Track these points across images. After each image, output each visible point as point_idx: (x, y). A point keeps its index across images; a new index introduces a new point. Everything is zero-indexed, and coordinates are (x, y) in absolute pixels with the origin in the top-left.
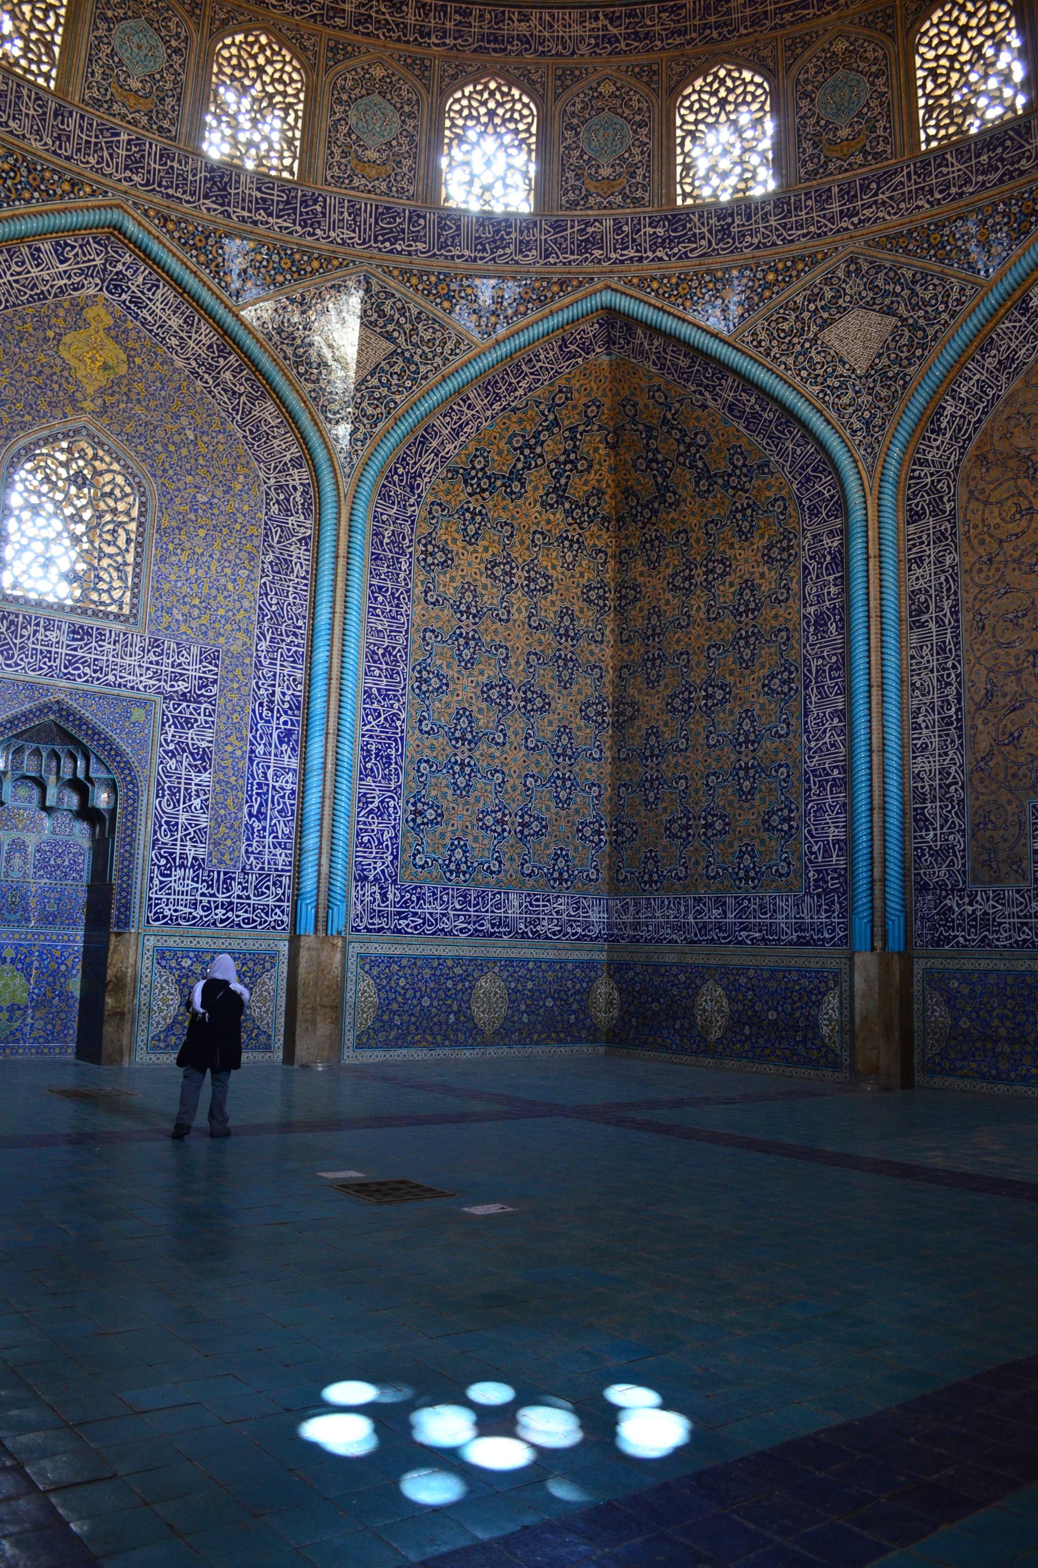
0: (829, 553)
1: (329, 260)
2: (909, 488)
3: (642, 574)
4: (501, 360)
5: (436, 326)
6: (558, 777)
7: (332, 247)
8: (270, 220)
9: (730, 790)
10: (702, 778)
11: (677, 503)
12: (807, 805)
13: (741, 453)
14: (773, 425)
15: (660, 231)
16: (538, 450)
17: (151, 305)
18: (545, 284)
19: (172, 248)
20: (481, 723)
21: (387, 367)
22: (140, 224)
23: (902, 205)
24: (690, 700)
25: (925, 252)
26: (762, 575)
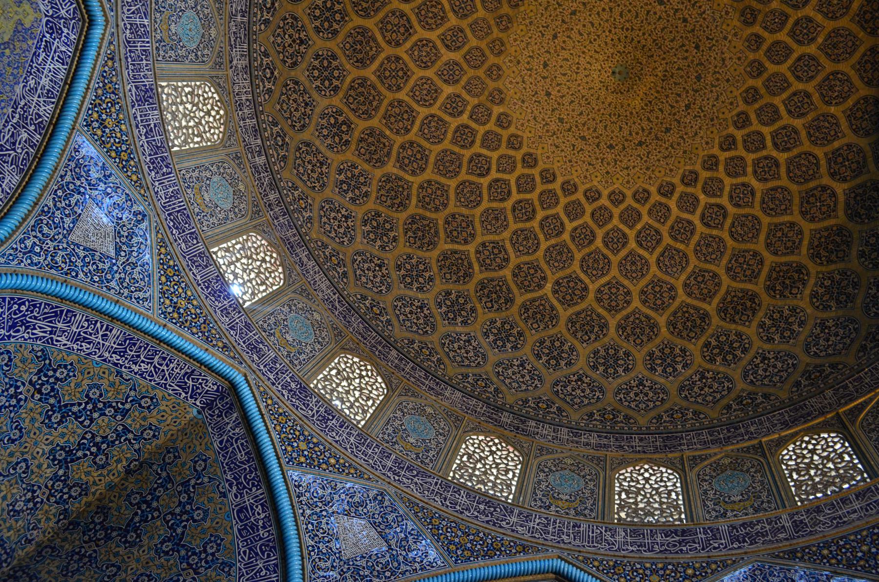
1: (141, 186)
4: (154, 336)
7: (150, 185)
8: (143, 137)
11: (132, 545)
13: (219, 545)
15: (293, 385)
16: (95, 415)
17: (50, 59)
18: (217, 336)
19: (98, 66)
22: (102, 39)
23: (426, 492)
25: (426, 523)
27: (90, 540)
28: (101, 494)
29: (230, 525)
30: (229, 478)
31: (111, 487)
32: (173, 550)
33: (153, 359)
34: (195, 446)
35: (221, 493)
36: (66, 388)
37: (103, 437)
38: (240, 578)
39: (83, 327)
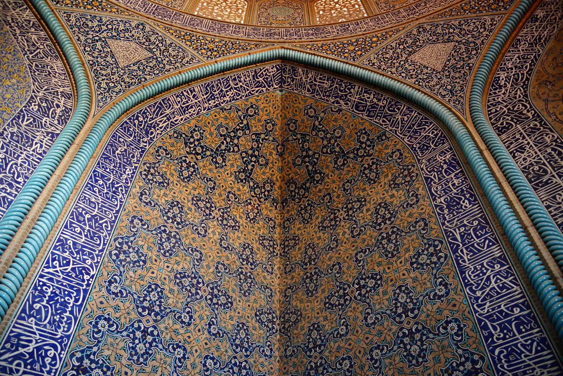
0: (445, 163)
2: (491, 119)
3: (299, 229)
5: (180, 50)
6: (235, 364)
9: (397, 359)
10: (365, 354)
11: (322, 179)
12: (493, 352)
13: (366, 132)
14: (386, 108)
16: (236, 141)
20: (170, 301)
21: (145, 63)
24: (345, 294)
26: (392, 196)
27: (300, 199)
28: (280, 177)
29: (360, 119)
30: (333, 101)
31: (281, 170)
32: (345, 160)
33: (230, 85)
34: (298, 107)
35: (337, 111)
36: (207, 141)
37: (251, 149)
38: (396, 134)
39: (179, 102)
